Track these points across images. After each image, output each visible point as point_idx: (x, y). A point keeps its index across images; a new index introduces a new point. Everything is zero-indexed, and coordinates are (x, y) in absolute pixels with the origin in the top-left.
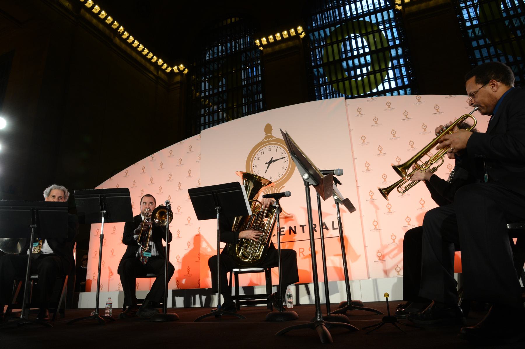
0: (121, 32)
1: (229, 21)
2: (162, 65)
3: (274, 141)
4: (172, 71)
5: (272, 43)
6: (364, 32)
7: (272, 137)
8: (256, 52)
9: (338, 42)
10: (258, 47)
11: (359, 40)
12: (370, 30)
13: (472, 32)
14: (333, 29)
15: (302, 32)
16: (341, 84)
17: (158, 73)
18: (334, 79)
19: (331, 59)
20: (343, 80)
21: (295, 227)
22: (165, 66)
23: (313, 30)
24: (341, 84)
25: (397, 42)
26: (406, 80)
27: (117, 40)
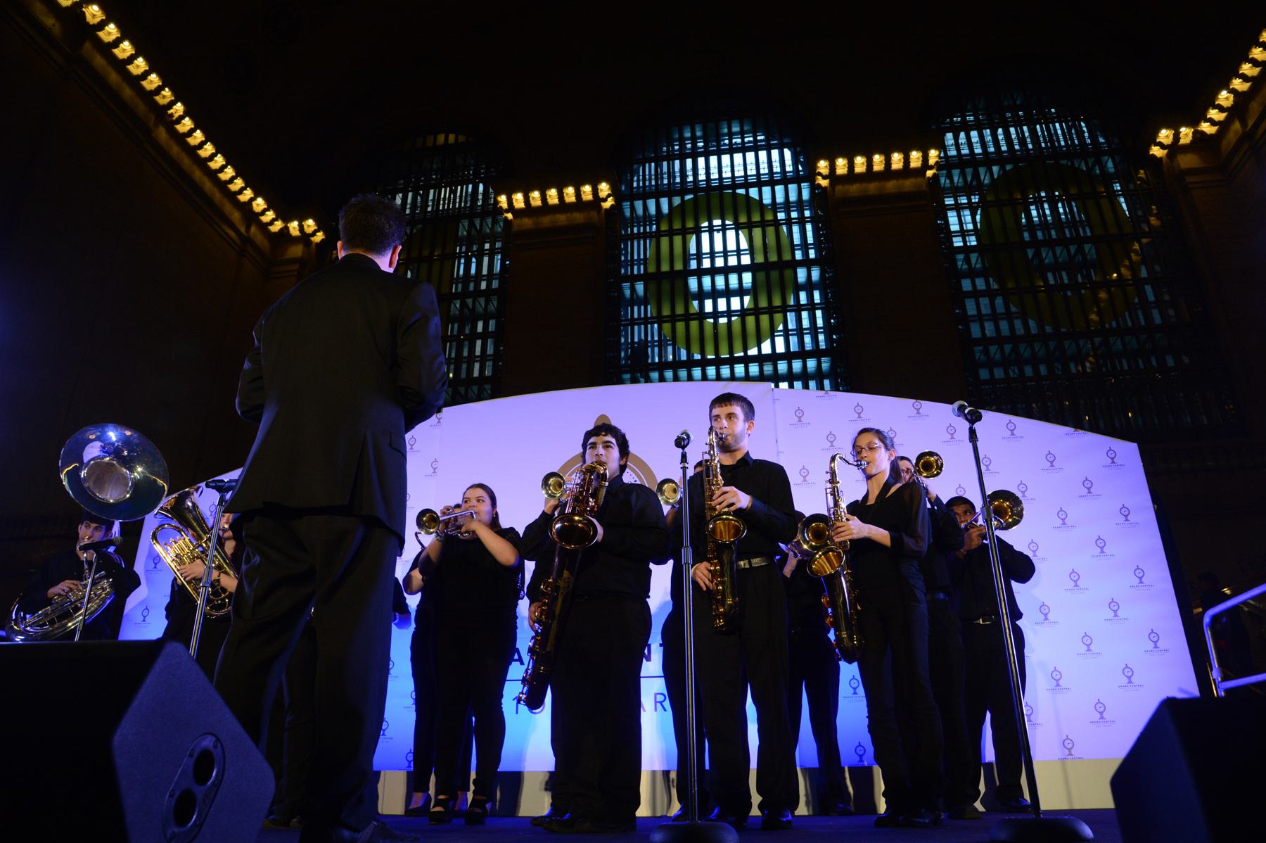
0: (176, 115)
1: (441, 138)
2: (263, 212)
4: (286, 229)
5: (537, 208)
6: (743, 219)
8: (495, 222)
9: (684, 233)
10: (501, 211)
11: (731, 234)
12: (756, 218)
14: (677, 201)
15: (609, 196)
16: (680, 326)
17: (248, 229)
18: (666, 312)
19: (665, 267)
20: (687, 317)
22: (270, 215)
23: (632, 197)
24: (680, 326)
25: (812, 254)
26: (821, 337)
27: (162, 134)
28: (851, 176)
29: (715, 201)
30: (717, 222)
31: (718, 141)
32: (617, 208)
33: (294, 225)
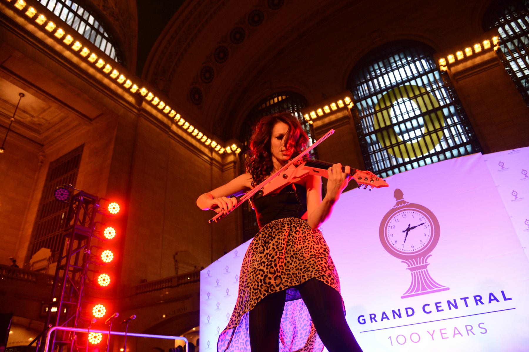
1: (276, 100)
3: (407, 206)
7: (404, 202)
9: (387, 108)
10: (307, 122)
11: (408, 103)
12: (417, 93)
13: (526, 82)
14: (380, 96)
21: (455, 300)
22: (219, 147)
23: (360, 100)
26: (463, 137)
27: (174, 128)
28: (457, 62)
29: (397, 92)
30: (400, 100)
31: (391, 66)
32: (355, 106)
33: (228, 150)
